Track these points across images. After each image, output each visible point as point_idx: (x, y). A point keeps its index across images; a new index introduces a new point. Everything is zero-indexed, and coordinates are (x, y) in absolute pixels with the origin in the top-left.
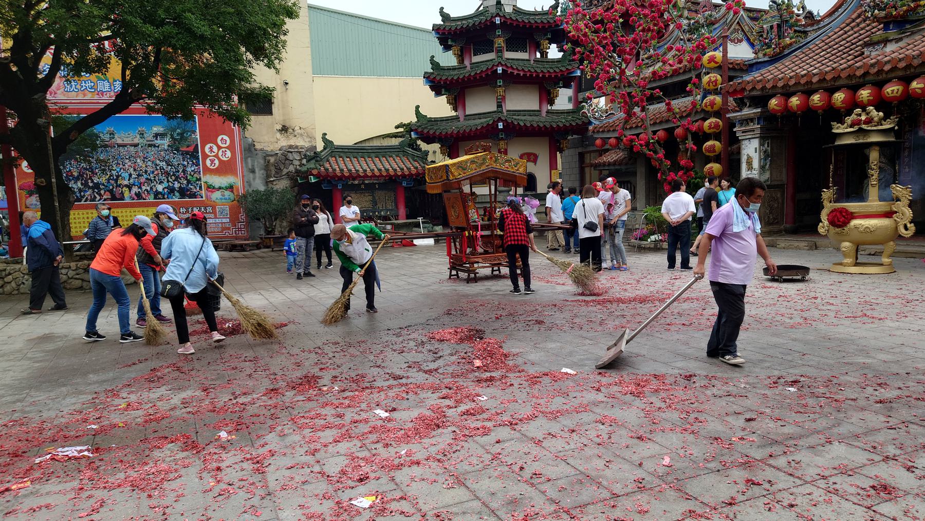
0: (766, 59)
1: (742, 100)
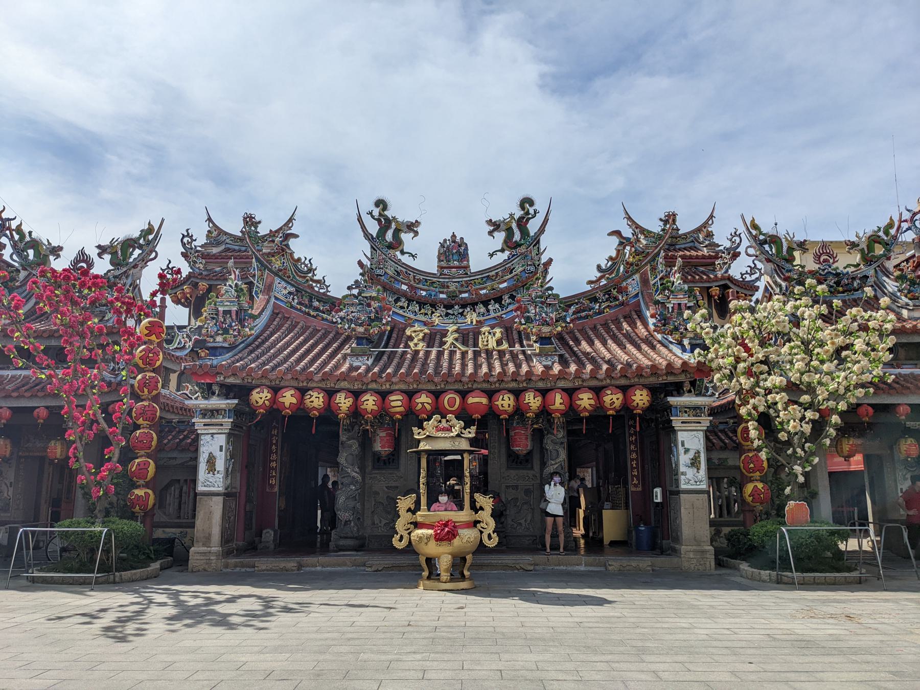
0: (226, 345)
1: (210, 386)
